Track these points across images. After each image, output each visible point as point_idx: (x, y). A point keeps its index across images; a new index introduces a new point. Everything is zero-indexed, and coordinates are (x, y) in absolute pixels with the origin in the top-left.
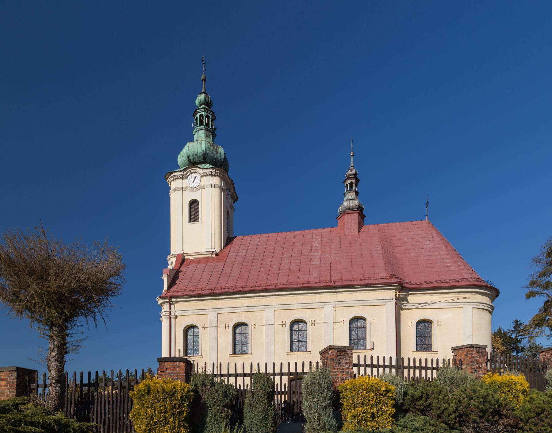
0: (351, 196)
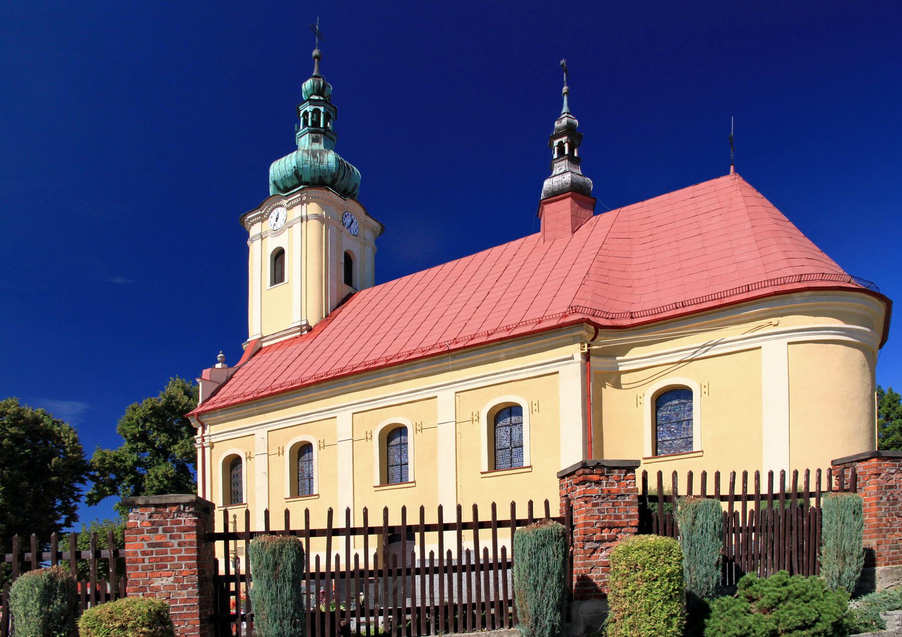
0: (560, 168)
